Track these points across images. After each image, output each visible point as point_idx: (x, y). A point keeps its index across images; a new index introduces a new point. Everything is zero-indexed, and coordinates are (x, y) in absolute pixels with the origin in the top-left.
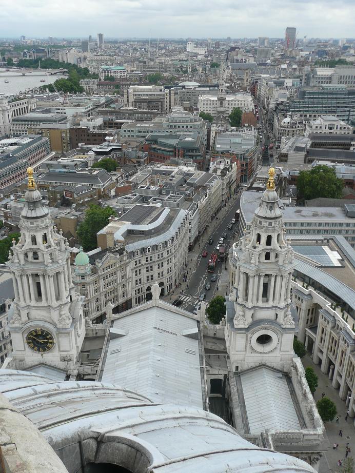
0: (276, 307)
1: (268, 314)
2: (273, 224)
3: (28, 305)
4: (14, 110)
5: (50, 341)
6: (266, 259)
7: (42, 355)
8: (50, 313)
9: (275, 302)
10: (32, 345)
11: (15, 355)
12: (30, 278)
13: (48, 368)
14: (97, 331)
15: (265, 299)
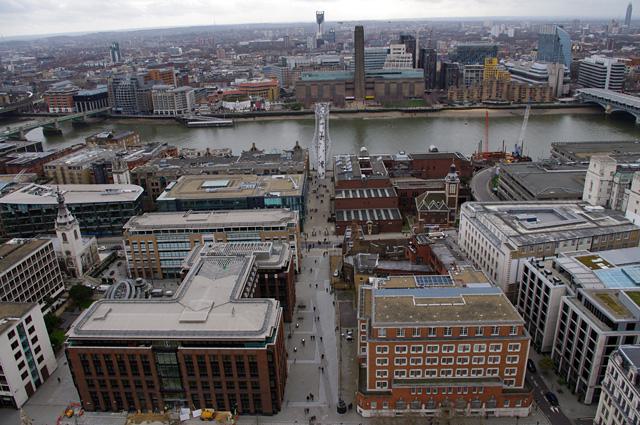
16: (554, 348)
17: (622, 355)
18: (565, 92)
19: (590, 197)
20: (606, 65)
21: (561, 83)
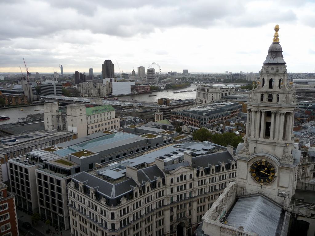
3: (257, 140)
4: (223, 94)
5: (272, 173)
7: (262, 186)
8: (275, 149)
10: (254, 174)
11: (237, 182)
12: (263, 115)
13: (265, 199)
14: (307, 185)
16: (40, 206)
17: (74, 181)
18: (35, 99)
19: (48, 126)
20: (53, 84)
21: (31, 94)
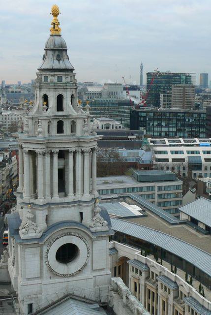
0: (79, 202)
1: (70, 214)
2: (64, 80)
6: (58, 133)
9: (77, 194)
15: (63, 194)
